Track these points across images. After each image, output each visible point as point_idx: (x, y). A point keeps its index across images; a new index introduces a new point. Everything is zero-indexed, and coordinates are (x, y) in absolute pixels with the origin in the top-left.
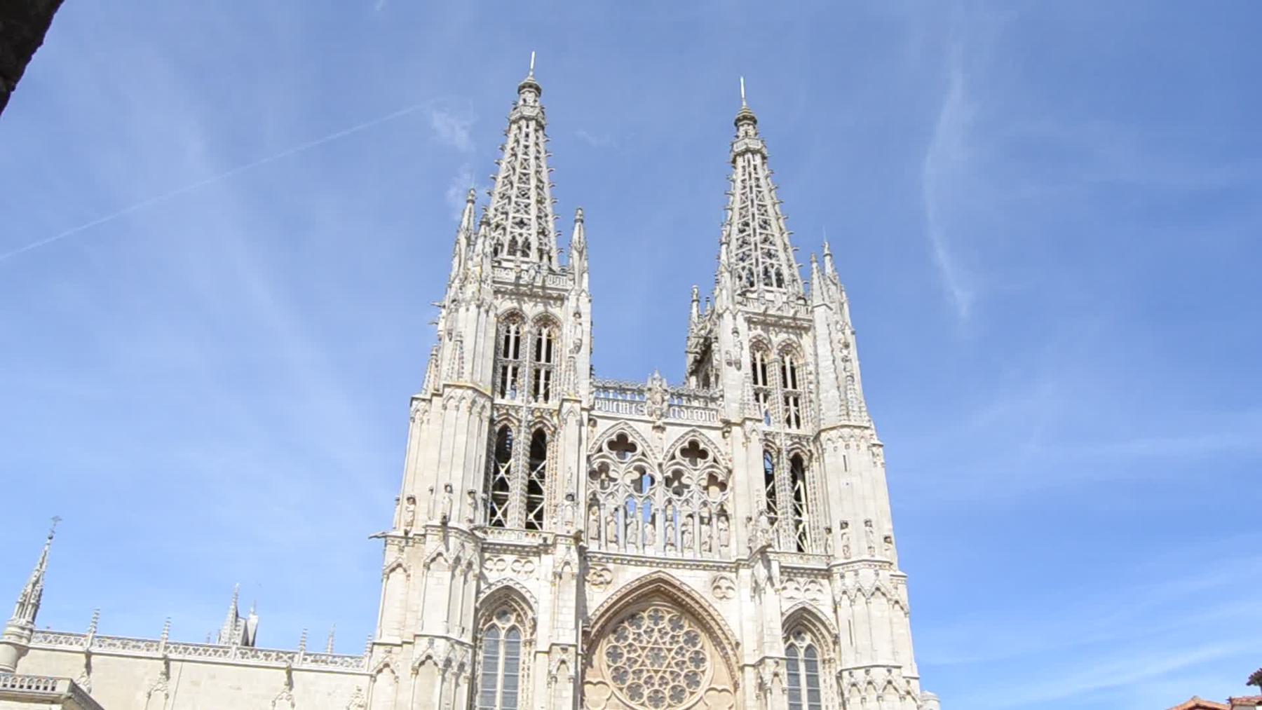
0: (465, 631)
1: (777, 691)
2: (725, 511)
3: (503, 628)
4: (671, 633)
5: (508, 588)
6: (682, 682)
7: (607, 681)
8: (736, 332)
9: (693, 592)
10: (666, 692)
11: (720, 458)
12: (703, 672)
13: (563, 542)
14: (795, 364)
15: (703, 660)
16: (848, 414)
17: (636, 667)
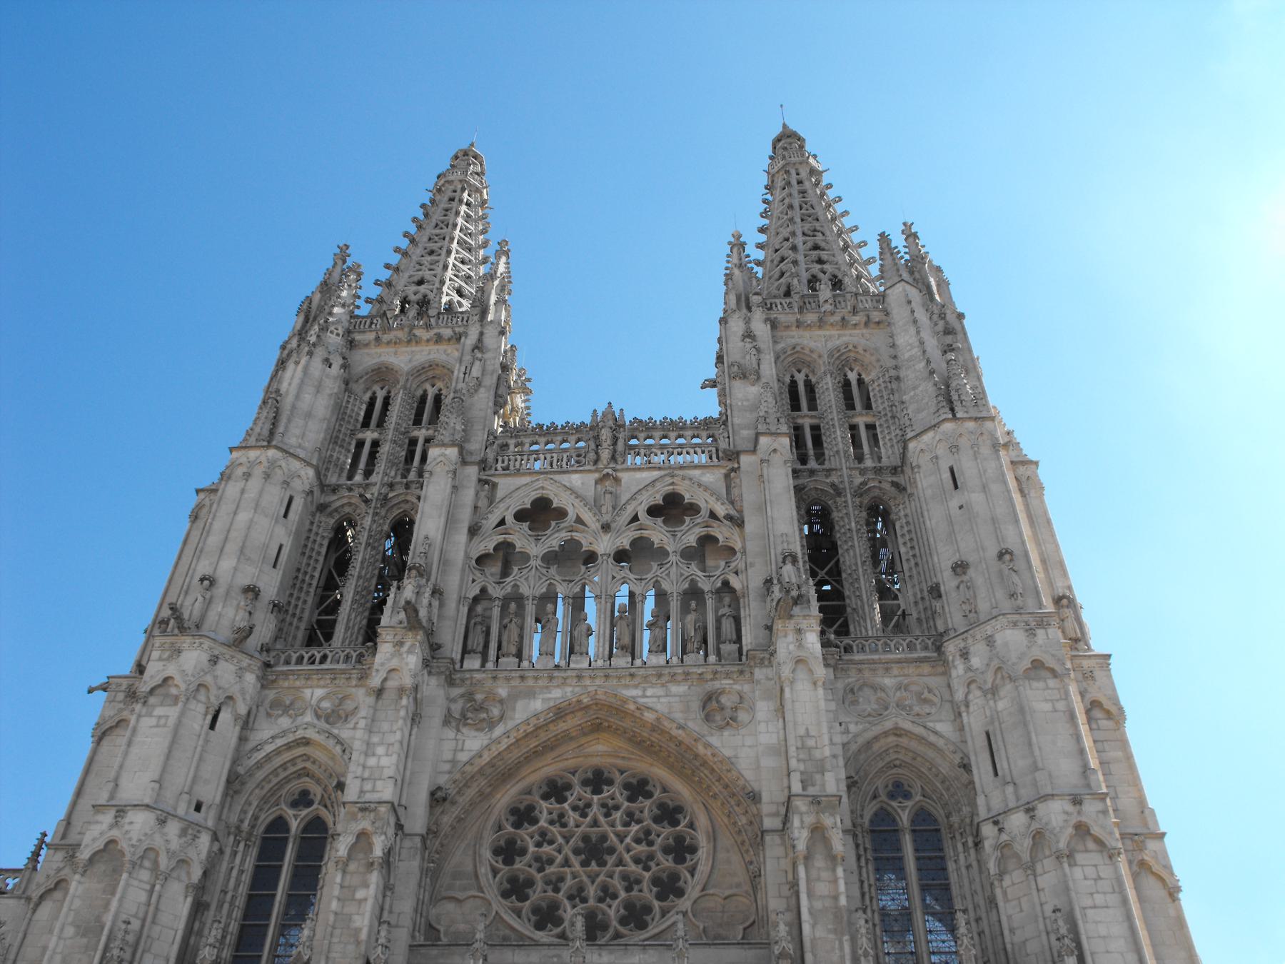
0: (203, 809)
1: (819, 862)
2: (733, 591)
3: (296, 817)
4: (626, 804)
5: (306, 742)
6: (647, 893)
7: (488, 897)
8: (749, 335)
9: (666, 723)
10: (612, 912)
11: (721, 510)
12: (692, 872)
13: (389, 638)
14: (867, 379)
15: (693, 850)
16: (952, 410)
17: (550, 870)
